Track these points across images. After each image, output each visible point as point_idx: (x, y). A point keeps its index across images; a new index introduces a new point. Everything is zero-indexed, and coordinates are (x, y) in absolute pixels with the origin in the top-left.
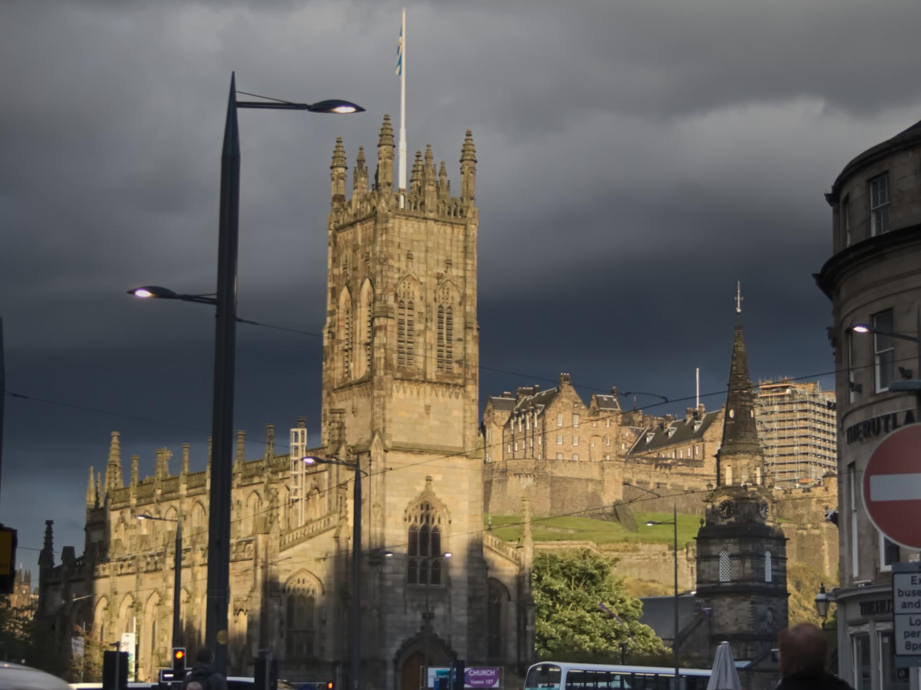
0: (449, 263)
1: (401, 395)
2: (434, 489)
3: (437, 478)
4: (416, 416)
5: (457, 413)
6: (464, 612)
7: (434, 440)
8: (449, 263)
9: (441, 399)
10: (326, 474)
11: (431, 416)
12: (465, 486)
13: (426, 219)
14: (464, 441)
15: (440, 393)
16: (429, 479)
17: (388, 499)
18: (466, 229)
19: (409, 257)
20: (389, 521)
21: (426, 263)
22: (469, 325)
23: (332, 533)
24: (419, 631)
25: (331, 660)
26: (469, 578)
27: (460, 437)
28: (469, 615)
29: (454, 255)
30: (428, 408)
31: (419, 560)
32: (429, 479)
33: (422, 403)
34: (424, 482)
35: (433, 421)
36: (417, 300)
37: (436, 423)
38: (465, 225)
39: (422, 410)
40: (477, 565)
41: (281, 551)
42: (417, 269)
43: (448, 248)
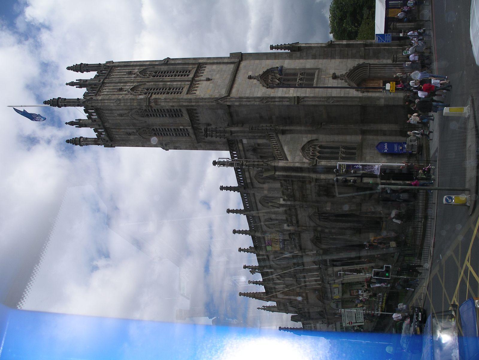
0: (130, 73)
1: (198, 93)
2: (257, 75)
3: (250, 73)
4: (211, 85)
5: (214, 67)
6: (333, 61)
7: (228, 77)
8: (130, 73)
9: (205, 73)
10: (245, 141)
11: (213, 78)
12: (257, 62)
13: (103, 83)
14: (231, 63)
15: (201, 74)
16: (250, 77)
17: (259, 95)
18: (115, 66)
19: (121, 90)
20: (272, 95)
21: (126, 82)
22: (166, 62)
23: (280, 136)
24: (343, 81)
25: (360, 138)
26: (312, 59)
27: (228, 65)
28: (334, 58)
29: (127, 71)
30: (208, 79)
31: (298, 81)
32: (250, 77)
33: (205, 82)
34: (252, 80)
35: (216, 77)
36: (146, 87)
37: (218, 76)
38: (113, 66)
39: (209, 82)
40: (305, 54)
41: (287, 160)
42: (129, 86)
43: (123, 73)
